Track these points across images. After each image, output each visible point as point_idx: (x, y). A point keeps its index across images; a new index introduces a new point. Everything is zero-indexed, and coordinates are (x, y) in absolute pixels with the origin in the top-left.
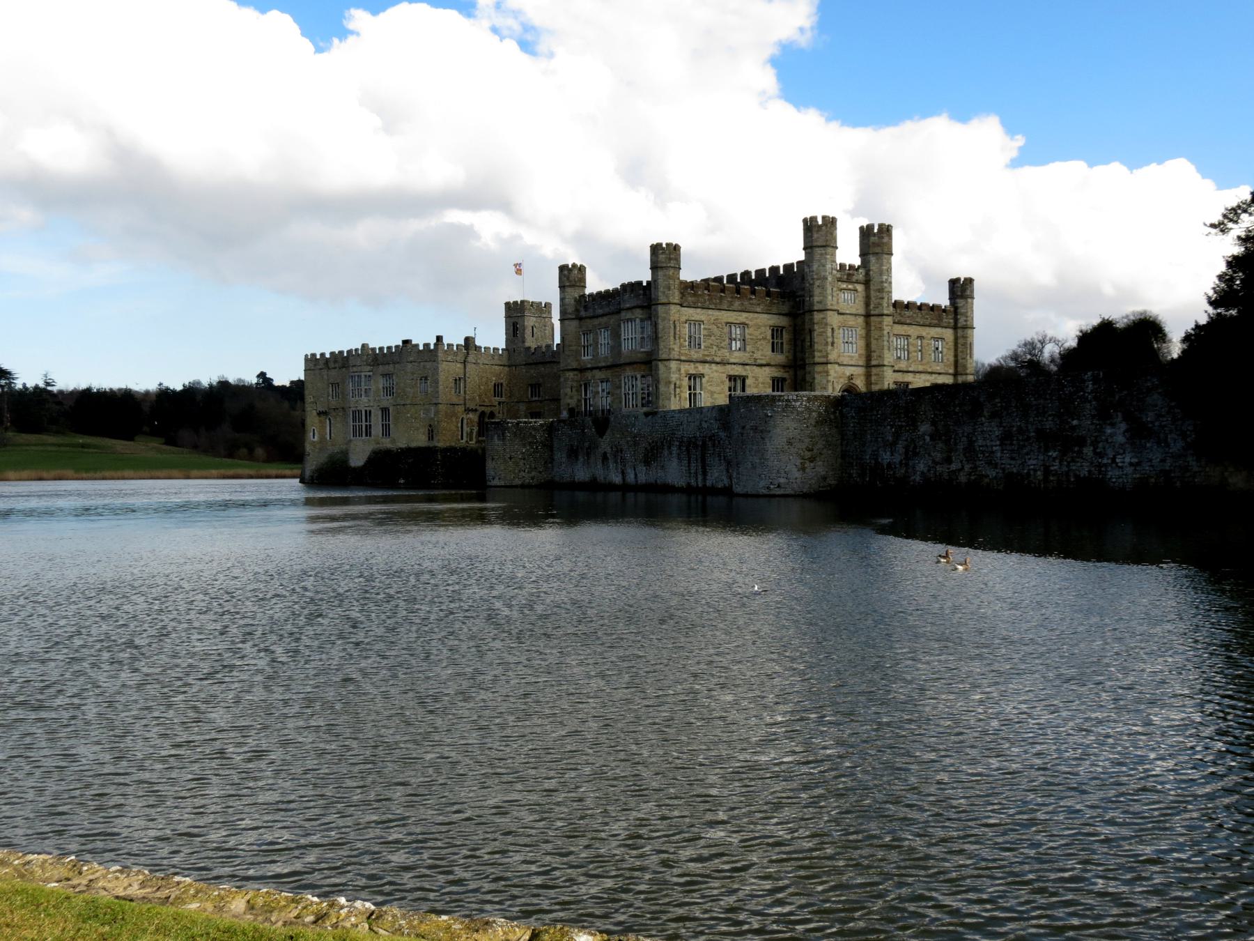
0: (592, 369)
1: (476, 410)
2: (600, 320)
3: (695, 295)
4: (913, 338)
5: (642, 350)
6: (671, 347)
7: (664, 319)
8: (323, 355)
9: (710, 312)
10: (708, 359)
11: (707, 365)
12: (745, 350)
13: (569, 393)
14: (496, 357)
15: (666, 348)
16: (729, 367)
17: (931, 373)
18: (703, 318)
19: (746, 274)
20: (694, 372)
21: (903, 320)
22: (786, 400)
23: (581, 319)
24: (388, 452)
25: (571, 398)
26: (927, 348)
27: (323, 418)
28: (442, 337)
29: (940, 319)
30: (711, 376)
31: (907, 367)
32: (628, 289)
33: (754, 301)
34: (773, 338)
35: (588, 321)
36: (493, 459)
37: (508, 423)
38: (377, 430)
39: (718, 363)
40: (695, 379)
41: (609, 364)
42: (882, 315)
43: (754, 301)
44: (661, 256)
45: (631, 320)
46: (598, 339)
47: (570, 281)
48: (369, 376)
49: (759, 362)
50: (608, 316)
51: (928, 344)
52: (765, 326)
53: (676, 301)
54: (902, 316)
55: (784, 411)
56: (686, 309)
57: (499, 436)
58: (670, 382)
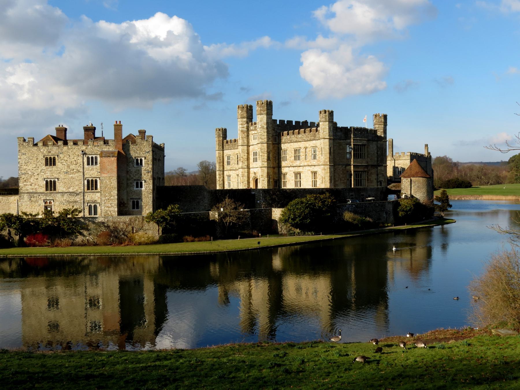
3: (228, 145)
4: (302, 148)
9: (232, 150)
10: (232, 169)
11: (231, 171)
17: (311, 166)
18: (231, 153)
21: (298, 140)
26: (309, 153)
29: (315, 136)
31: (300, 164)
42: (242, 145)
51: (309, 151)
54: (297, 138)
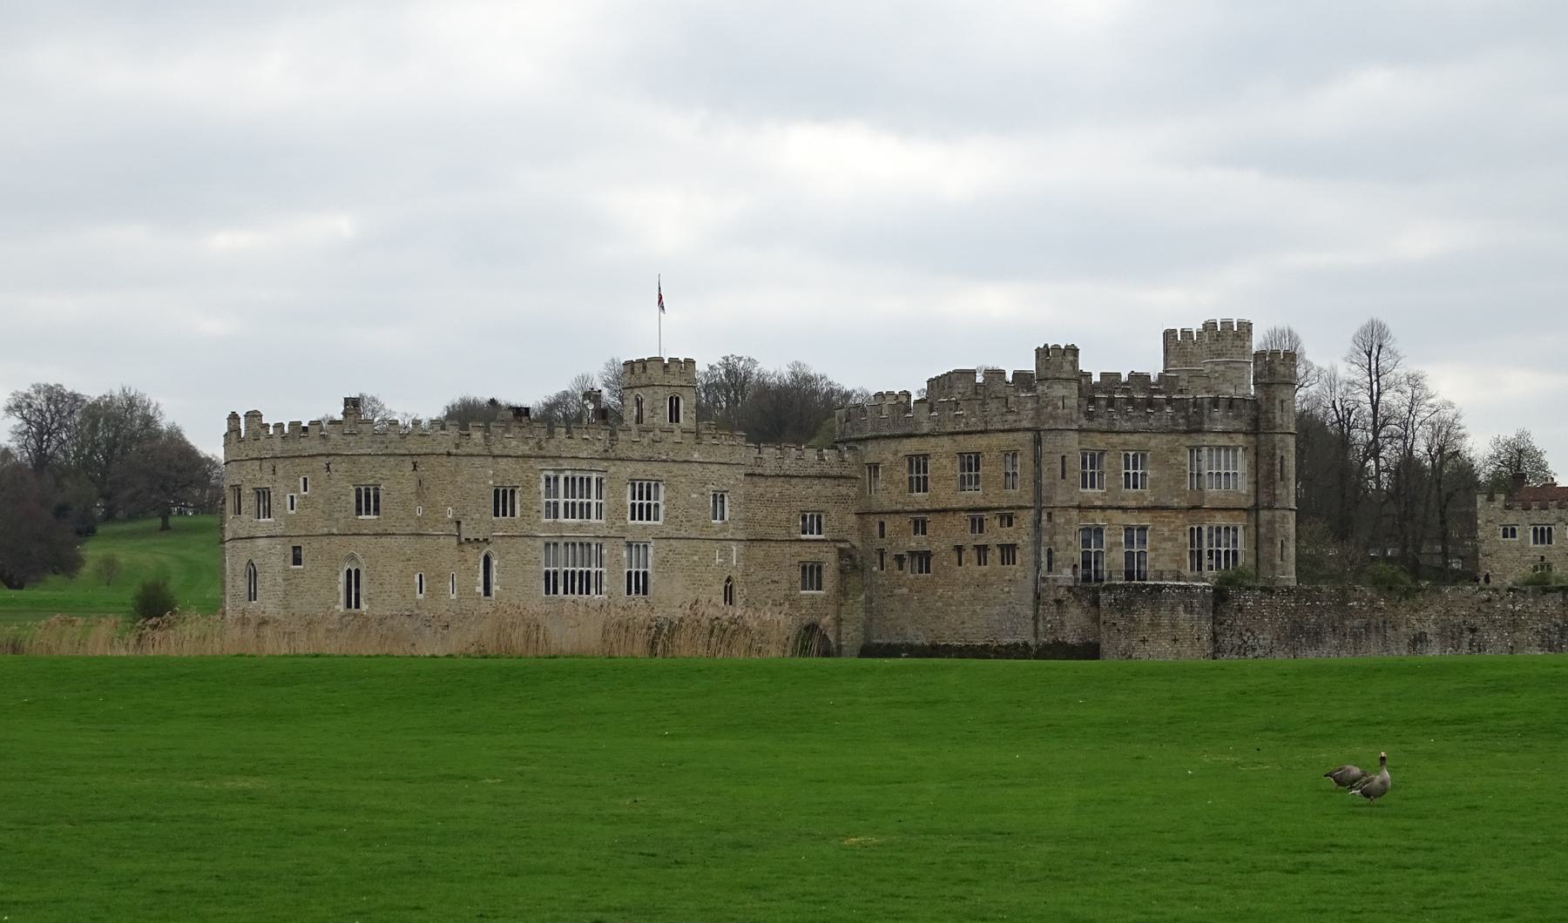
0: (1102, 508)
2: (1127, 437)
23: (1080, 430)
25: (1075, 550)
27: (468, 548)
35: (1096, 434)
46: (1119, 464)
50: (1149, 435)
57: (1186, 607)
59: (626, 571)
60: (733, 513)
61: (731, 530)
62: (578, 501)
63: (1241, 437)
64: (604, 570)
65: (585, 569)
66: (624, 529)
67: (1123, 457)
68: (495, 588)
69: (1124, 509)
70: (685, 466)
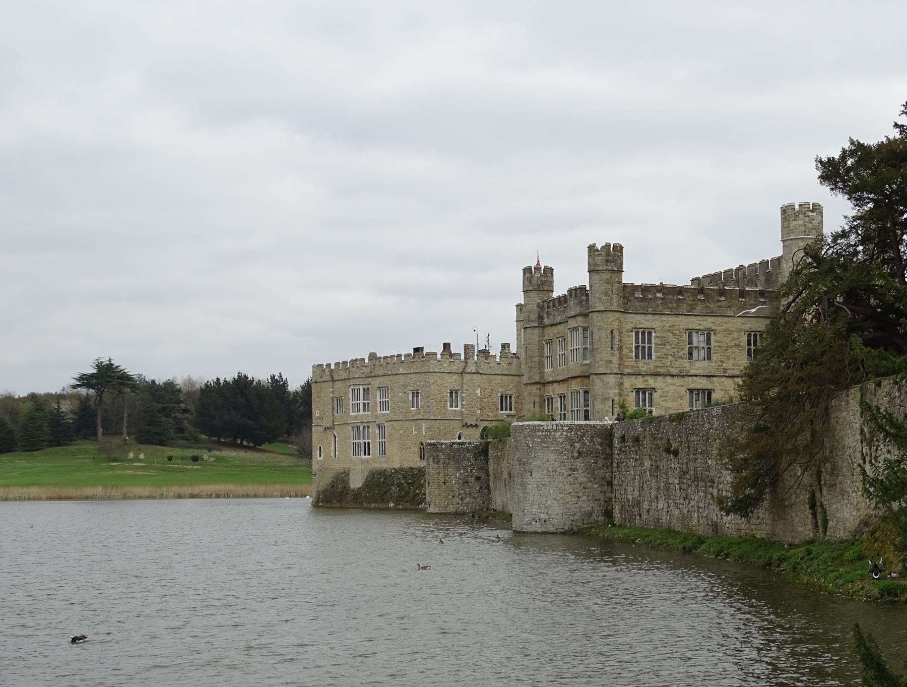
0: (553, 382)
1: (476, 426)
3: (643, 299)
5: (585, 362)
6: (608, 359)
7: (600, 329)
8: (329, 365)
9: (664, 318)
10: (661, 371)
11: (660, 378)
12: (709, 358)
13: (532, 409)
14: (504, 364)
15: (601, 360)
16: (687, 379)
18: (655, 325)
19: (741, 268)
20: (643, 386)
22: (546, 431)
23: (543, 327)
24: (381, 472)
28: (449, 344)
30: (666, 390)
32: (573, 294)
33: (724, 303)
34: (749, 344)
35: (550, 328)
36: (429, 484)
37: (442, 444)
38: (375, 449)
39: (673, 376)
40: (644, 393)
41: (565, 377)
43: (724, 303)
44: (596, 258)
45: (575, 329)
46: (557, 349)
47: (534, 285)
48: (368, 389)
49: (730, 373)
52: (739, 331)
53: (614, 308)
55: (543, 441)
56: (631, 315)
58: (607, 399)
59: (378, 440)
60: (423, 403)
61: (422, 413)
62: (384, 400)
63: (579, 319)
64: (370, 441)
65: (358, 441)
66: (377, 417)
67: (558, 342)
68: (337, 453)
69: (559, 382)
70: (397, 377)
